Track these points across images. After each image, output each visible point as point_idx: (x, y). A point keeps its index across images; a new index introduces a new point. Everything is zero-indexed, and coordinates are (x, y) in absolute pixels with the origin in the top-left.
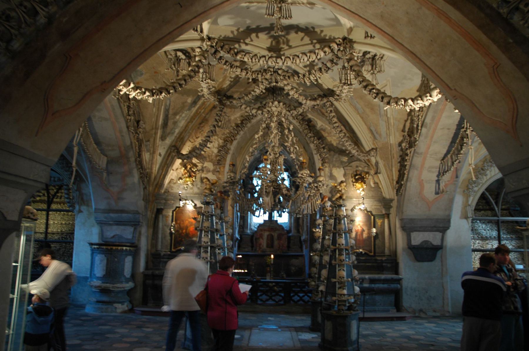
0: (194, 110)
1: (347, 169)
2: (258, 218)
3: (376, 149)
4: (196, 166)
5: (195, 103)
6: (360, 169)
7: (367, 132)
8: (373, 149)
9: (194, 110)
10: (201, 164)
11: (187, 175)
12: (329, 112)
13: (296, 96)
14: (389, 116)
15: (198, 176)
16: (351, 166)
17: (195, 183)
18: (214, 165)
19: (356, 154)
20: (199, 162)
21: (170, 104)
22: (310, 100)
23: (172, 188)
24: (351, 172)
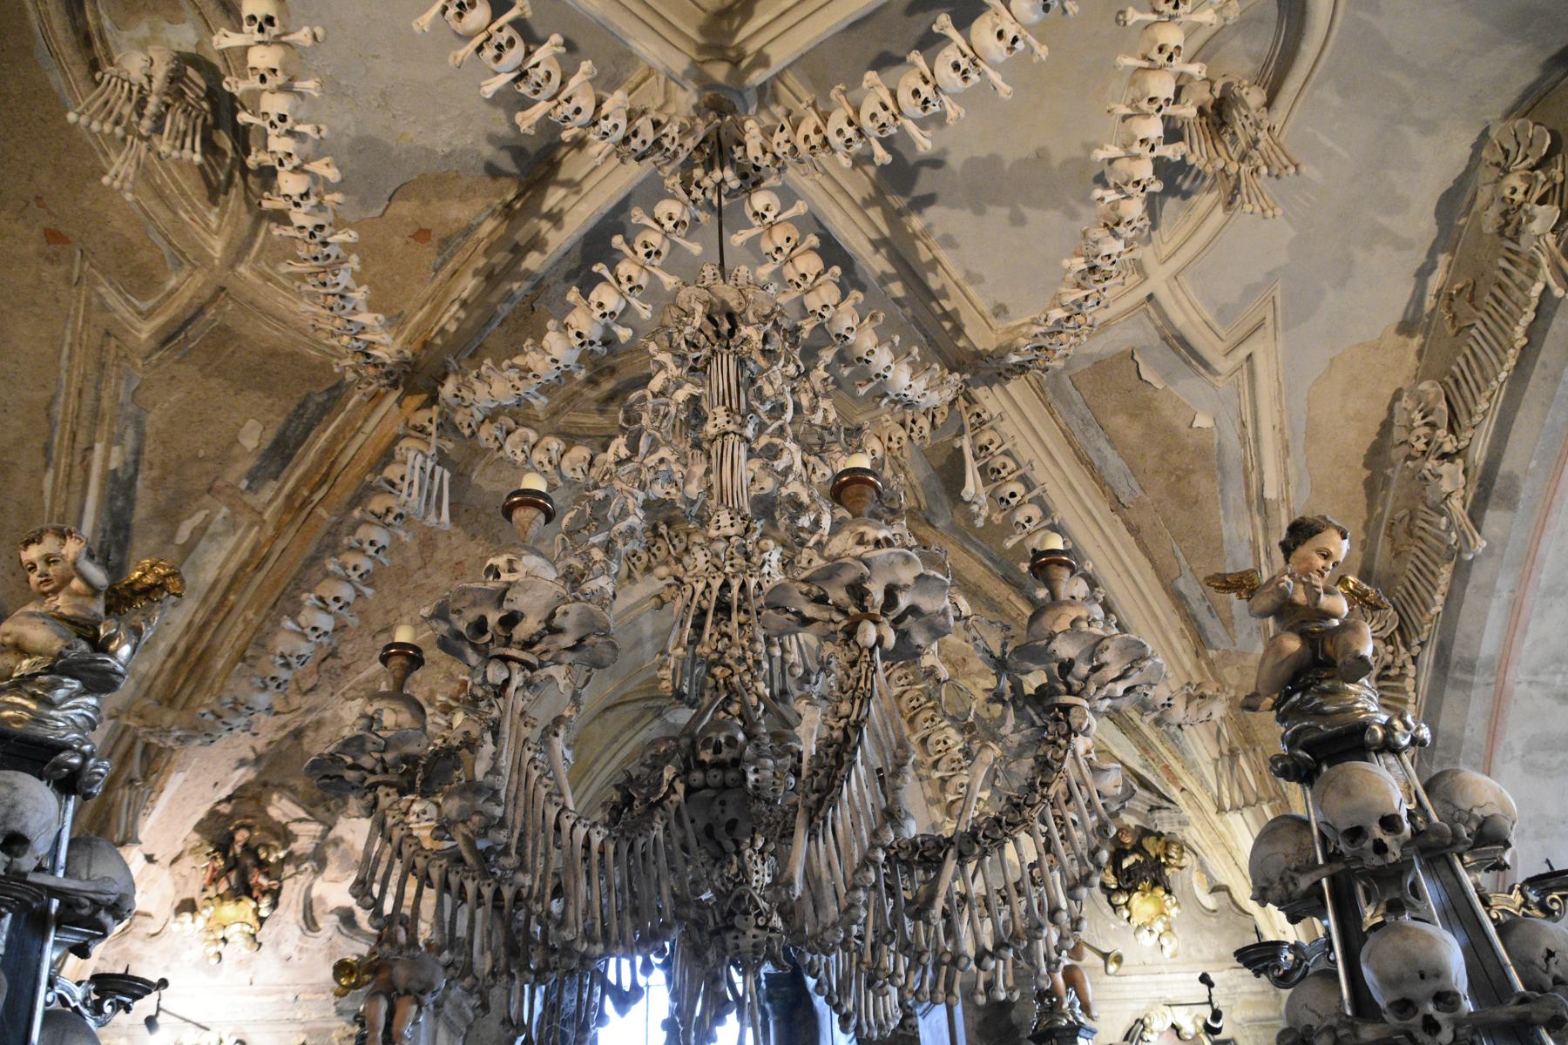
5: (280, 452)
6: (1131, 821)
7: (1161, 604)
10: (315, 828)
11: (223, 886)
15: (292, 892)
17: (265, 934)
20: (302, 814)
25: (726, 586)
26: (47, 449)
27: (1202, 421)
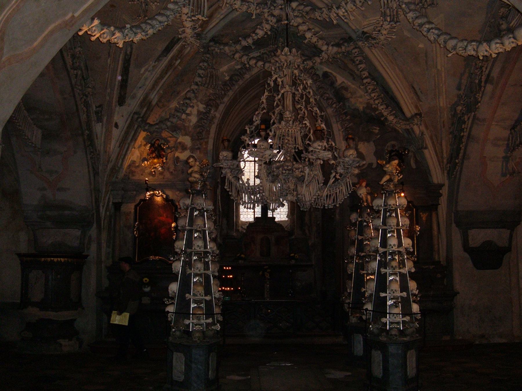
0: (165, 61)
2: (247, 215)
3: (420, 115)
4: (168, 142)
8: (416, 114)
9: (165, 61)
12: (357, 62)
13: (314, 39)
14: (439, 67)
15: (170, 156)
18: (192, 140)
19: (394, 121)
21: (131, 53)
22: (332, 45)
23: (133, 173)
25: (288, 131)
26: (109, 53)
27: (421, 46)
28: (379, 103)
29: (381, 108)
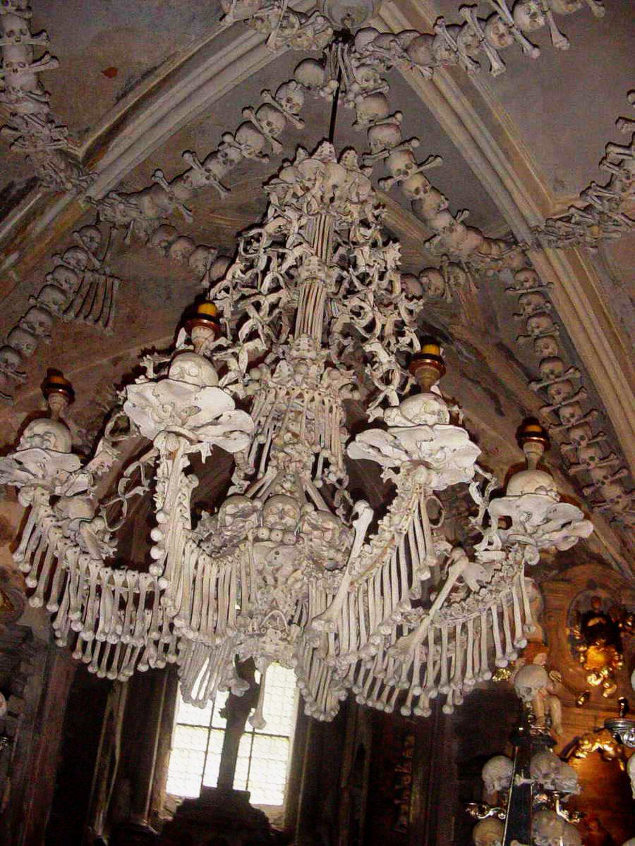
1: (556, 591)
16: (568, 581)
24: (567, 603)
28: (582, 438)
29: (585, 455)
